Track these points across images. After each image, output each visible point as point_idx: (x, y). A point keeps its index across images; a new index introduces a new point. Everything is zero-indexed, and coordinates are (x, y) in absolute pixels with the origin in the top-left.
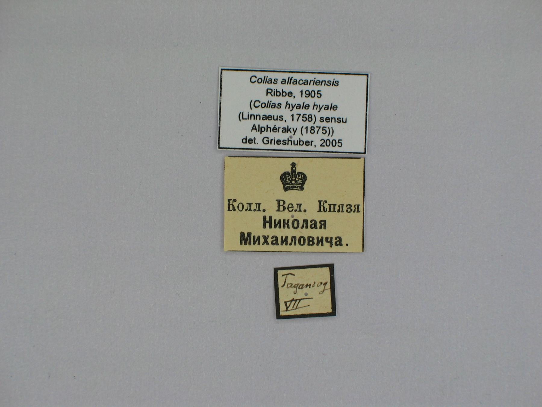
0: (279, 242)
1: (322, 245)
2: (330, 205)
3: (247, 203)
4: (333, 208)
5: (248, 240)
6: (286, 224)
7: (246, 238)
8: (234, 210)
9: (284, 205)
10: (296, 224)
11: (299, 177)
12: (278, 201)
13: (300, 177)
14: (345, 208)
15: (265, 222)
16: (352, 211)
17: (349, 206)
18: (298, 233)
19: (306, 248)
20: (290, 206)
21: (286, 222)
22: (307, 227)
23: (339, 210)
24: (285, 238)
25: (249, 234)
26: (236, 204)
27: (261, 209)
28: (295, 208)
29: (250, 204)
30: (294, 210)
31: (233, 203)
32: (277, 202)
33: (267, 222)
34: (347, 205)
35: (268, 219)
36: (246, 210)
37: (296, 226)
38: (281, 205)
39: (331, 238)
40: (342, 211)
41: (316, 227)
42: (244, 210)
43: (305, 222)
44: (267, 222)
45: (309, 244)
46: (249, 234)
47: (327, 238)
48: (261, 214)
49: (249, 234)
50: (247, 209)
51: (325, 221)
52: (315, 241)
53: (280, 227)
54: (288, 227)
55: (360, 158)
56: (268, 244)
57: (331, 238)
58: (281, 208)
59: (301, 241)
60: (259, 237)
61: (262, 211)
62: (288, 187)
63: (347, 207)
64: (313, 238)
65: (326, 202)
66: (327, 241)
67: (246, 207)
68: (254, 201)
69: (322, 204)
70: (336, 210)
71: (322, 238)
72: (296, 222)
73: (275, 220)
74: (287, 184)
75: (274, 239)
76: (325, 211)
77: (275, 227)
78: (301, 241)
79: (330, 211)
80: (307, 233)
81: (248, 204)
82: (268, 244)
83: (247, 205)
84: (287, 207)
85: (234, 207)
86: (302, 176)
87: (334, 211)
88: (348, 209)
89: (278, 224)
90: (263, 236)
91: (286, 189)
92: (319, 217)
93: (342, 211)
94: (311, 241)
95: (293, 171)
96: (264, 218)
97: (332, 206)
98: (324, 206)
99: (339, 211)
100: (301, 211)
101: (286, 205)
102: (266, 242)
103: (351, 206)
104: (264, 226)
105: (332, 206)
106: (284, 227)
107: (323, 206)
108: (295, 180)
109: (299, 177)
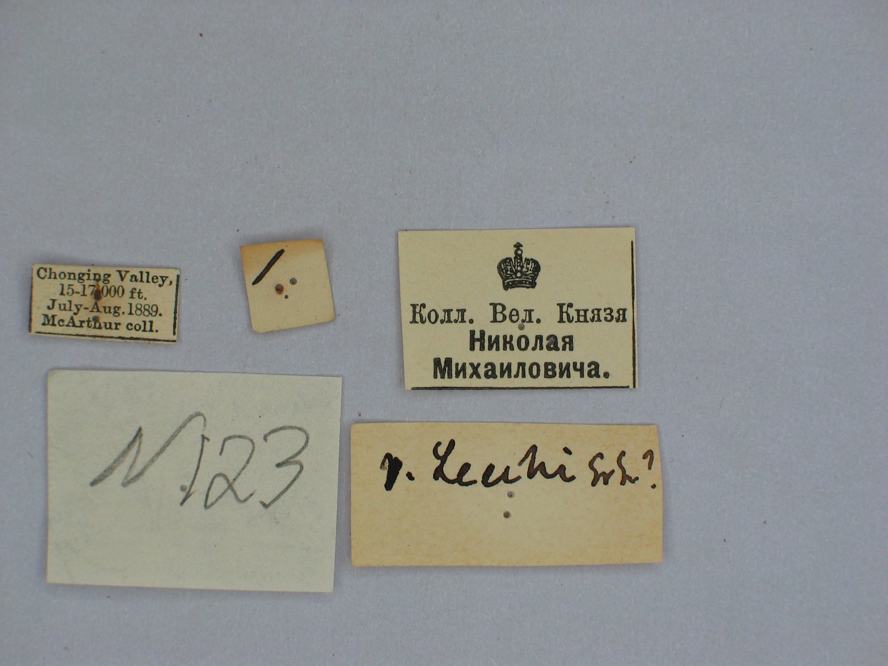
1: (569, 376)
2: (578, 311)
3: (525, 310)
4: (583, 316)
5: (438, 370)
6: (508, 342)
7: (443, 367)
8: (423, 322)
12: (494, 305)
13: (529, 266)
14: (603, 315)
15: (473, 340)
18: (529, 357)
19: (542, 381)
20: (514, 313)
21: (508, 339)
22: (541, 348)
23: (594, 317)
24: (566, 365)
25: (448, 361)
26: (425, 312)
27: (467, 318)
29: (448, 311)
32: (492, 307)
33: (478, 340)
35: (477, 336)
37: (523, 346)
38: (498, 311)
40: (599, 320)
41: (556, 348)
44: (477, 340)
45: (547, 376)
46: (438, 362)
48: (466, 328)
50: (443, 319)
51: (571, 337)
52: (557, 370)
53: (498, 349)
54: (512, 348)
56: (479, 376)
57: (582, 364)
60: (464, 365)
62: (510, 282)
64: (554, 365)
67: (441, 315)
70: (588, 319)
73: (490, 337)
75: (489, 367)
76: (570, 321)
77: (490, 348)
78: (532, 370)
79: (579, 321)
80: (543, 356)
82: (479, 376)
83: (525, 312)
87: (586, 321)
88: (607, 316)
89: (494, 343)
91: (506, 287)
92: (562, 331)
93: (599, 320)
95: (518, 257)
96: (472, 333)
97: (582, 313)
98: (568, 312)
99: (592, 320)
100: (465, 322)
101: (507, 313)
102: (475, 373)
104: (472, 348)
105: (582, 313)
106: (505, 348)
108: (521, 271)
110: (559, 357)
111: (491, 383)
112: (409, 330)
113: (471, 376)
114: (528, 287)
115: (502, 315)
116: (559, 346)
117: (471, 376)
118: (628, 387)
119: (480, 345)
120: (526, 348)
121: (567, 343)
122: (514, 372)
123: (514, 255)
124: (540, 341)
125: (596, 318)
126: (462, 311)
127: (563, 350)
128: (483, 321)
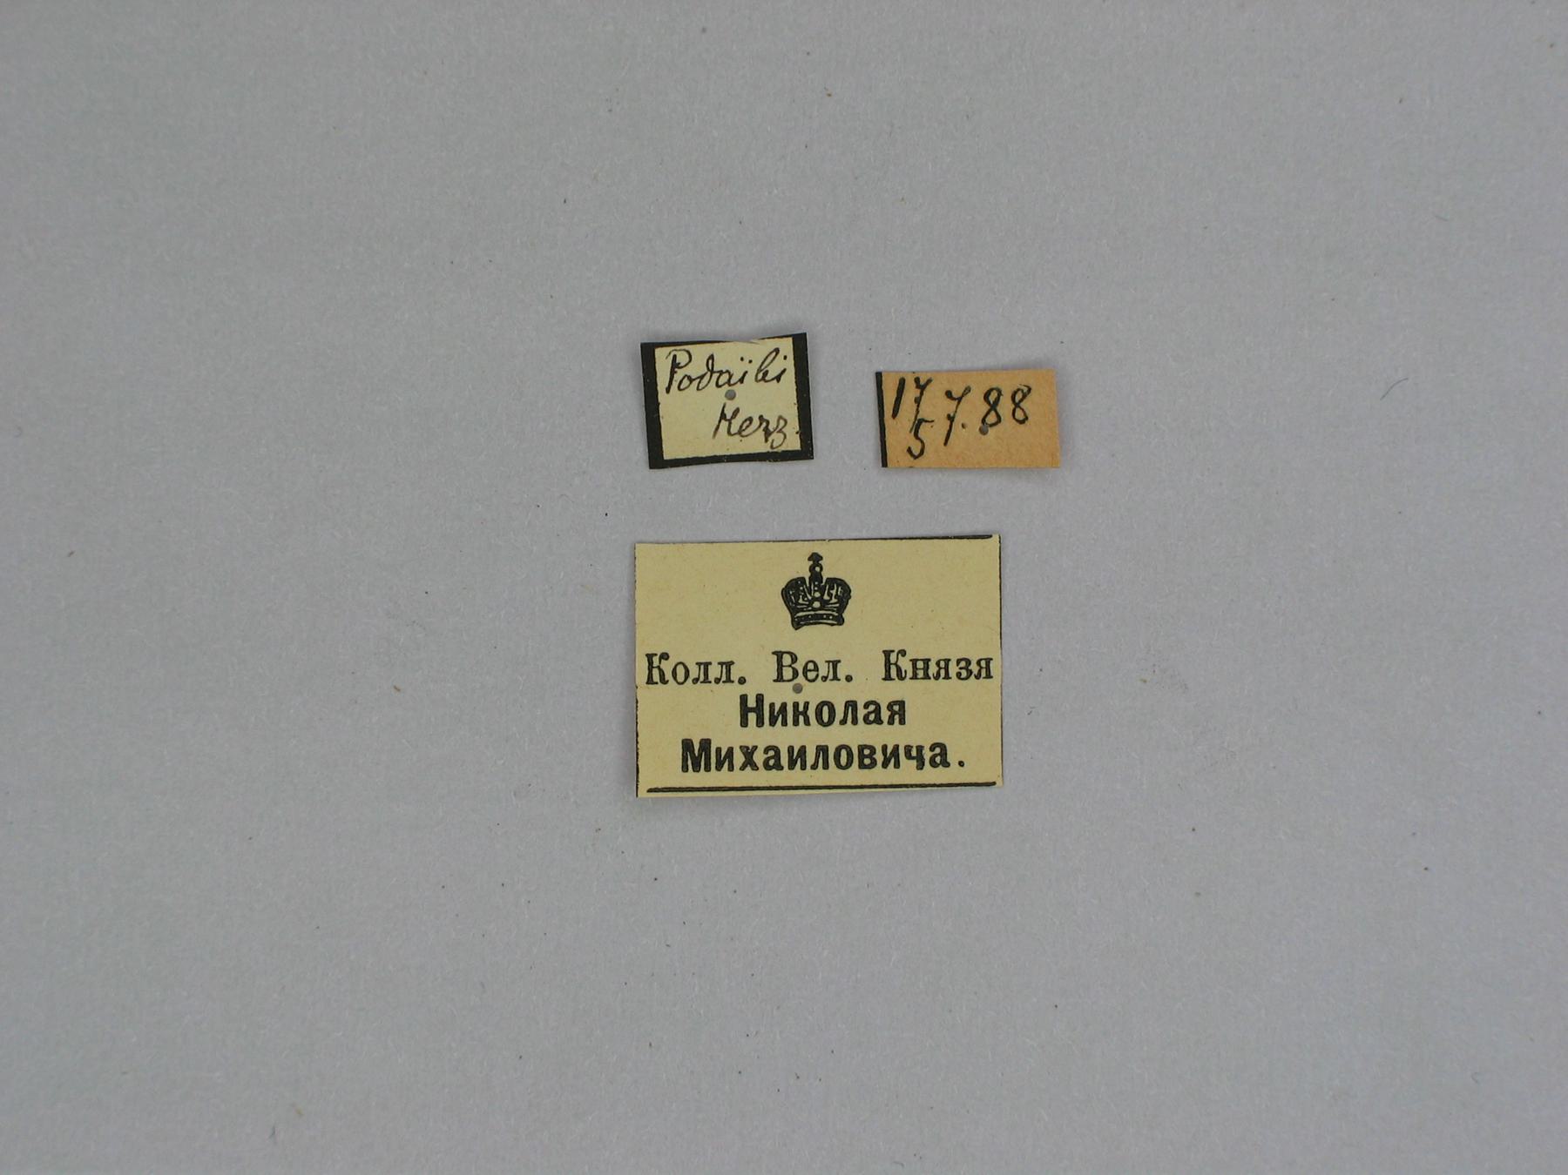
0: (784, 761)
1: (897, 765)
2: (914, 662)
4: (921, 669)
6: (800, 714)
7: (696, 755)
8: (664, 681)
10: (825, 714)
12: (779, 655)
13: (834, 592)
14: (953, 669)
15: (745, 710)
16: (973, 676)
17: (963, 664)
18: (835, 736)
19: (854, 775)
20: (811, 666)
21: (801, 708)
22: (855, 722)
24: (799, 750)
25: (705, 744)
27: (735, 676)
28: (823, 671)
30: (820, 678)
32: (776, 657)
33: (752, 710)
35: (752, 703)
36: (696, 681)
37: (826, 718)
39: (920, 749)
40: (947, 677)
41: (878, 721)
42: (690, 680)
43: (850, 708)
45: (862, 766)
47: (908, 749)
48: (736, 690)
49: (705, 744)
52: (879, 757)
53: (785, 723)
54: (807, 722)
55: (991, 536)
57: (920, 749)
59: (843, 757)
60: (730, 751)
65: (903, 653)
66: (909, 756)
68: (715, 657)
69: (893, 658)
71: (896, 748)
72: (825, 709)
74: (802, 610)
76: (901, 677)
77: (773, 723)
78: (843, 757)
79: (915, 677)
81: (699, 664)
82: (755, 767)
84: (800, 672)
85: (662, 674)
86: (840, 589)
87: (927, 677)
89: (778, 715)
90: (741, 747)
91: (797, 624)
92: (886, 693)
94: (866, 757)
95: (816, 576)
96: (744, 699)
97: (920, 665)
99: (937, 677)
101: (799, 666)
102: (749, 762)
103: (968, 662)
104: (744, 723)
105: (920, 665)
106: (796, 723)
107: (896, 664)
108: (821, 599)
111: (775, 778)
113: (743, 768)
114: (832, 625)
117: (743, 768)
120: (831, 722)
121: (896, 713)
122: (810, 759)
123: (809, 574)
125: (983, 673)
126: (728, 665)
128: (762, 682)
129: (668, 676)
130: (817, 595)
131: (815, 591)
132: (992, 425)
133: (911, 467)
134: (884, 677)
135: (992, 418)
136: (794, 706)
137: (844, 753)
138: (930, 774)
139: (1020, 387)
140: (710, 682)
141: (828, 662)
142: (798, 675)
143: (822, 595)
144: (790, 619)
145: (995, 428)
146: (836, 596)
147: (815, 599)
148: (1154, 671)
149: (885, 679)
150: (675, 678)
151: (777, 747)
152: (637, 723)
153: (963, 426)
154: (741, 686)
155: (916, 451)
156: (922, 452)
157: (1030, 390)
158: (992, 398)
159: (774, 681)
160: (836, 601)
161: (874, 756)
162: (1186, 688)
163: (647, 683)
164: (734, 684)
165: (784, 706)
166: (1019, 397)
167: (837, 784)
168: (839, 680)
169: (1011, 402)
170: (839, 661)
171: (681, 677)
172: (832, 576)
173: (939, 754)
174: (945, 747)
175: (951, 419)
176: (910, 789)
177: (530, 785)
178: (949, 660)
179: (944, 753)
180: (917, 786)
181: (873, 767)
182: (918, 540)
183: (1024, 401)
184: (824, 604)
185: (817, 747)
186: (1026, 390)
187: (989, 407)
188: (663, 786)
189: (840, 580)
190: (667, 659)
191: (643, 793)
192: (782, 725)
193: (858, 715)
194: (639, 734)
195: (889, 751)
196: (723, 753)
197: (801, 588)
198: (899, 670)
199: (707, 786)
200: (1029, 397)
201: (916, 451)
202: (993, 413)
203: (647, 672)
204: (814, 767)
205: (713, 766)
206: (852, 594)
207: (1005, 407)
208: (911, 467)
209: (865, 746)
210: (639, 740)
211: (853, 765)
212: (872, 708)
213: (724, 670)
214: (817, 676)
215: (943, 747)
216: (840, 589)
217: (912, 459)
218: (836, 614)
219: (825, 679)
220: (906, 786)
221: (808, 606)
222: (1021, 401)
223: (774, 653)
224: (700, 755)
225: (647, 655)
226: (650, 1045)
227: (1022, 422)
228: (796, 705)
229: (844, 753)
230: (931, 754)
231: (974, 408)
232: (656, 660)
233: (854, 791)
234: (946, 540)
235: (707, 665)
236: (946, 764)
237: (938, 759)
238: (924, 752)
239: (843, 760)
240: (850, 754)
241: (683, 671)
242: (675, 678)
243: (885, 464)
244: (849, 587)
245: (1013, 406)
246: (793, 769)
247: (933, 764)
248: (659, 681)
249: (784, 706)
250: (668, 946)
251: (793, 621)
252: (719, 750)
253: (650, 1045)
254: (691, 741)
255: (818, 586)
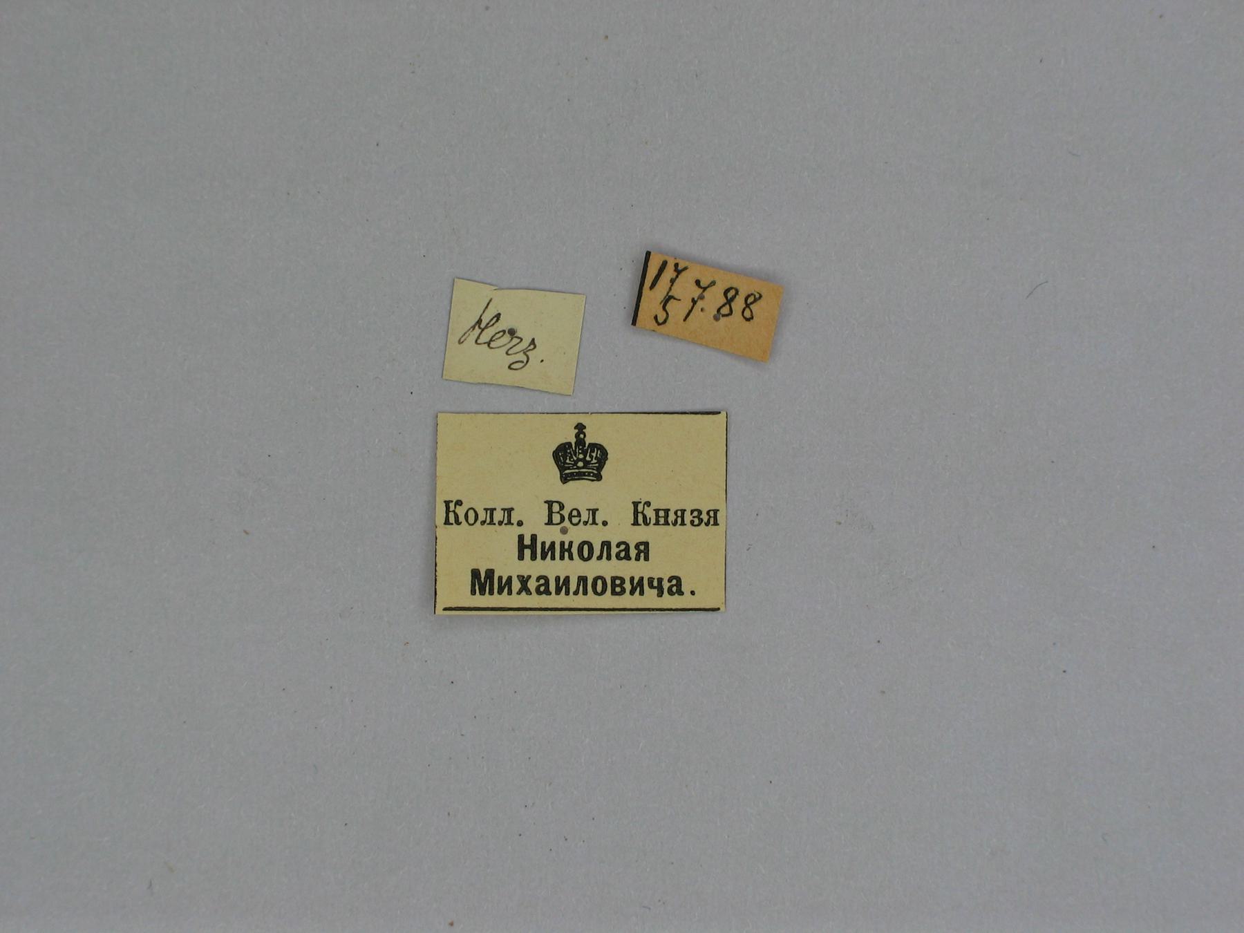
1: (642, 593)
2: (657, 511)
4: (663, 517)
6: (566, 550)
7: (482, 581)
8: (458, 522)
9: (561, 512)
10: (585, 551)
11: (593, 454)
12: (550, 504)
13: (594, 455)
14: (688, 518)
15: (521, 547)
16: (703, 523)
17: (695, 514)
18: (593, 569)
19: (608, 600)
20: (575, 513)
21: (566, 546)
22: (609, 558)
25: (490, 573)
26: (461, 511)
27: (514, 520)
28: (584, 517)
30: (582, 523)
31: (455, 508)
32: (547, 505)
33: (527, 547)
34: (692, 512)
35: (527, 541)
36: (483, 523)
37: (586, 554)
39: (660, 580)
40: (683, 523)
41: (628, 557)
42: (479, 522)
43: (605, 547)
45: (614, 593)
47: (651, 580)
48: (515, 531)
49: (490, 573)
51: (646, 544)
52: (628, 586)
53: (553, 558)
54: (571, 558)
55: (720, 413)
57: (660, 580)
58: (556, 518)
59: (599, 585)
60: (510, 579)
61: (515, 524)
63: (691, 514)
65: (648, 504)
66: (651, 586)
68: (499, 505)
69: (640, 508)
70: (670, 522)
71: (641, 579)
72: (586, 547)
74: (569, 468)
76: (646, 523)
77: (544, 557)
78: (599, 585)
79: (657, 523)
81: (486, 510)
82: (529, 592)
86: (599, 452)
87: (667, 523)
89: (548, 551)
90: (518, 576)
91: (565, 479)
92: (634, 535)
94: (617, 585)
95: (580, 442)
96: (521, 538)
97: (662, 513)
99: (675, 523)
101: (566, 513)
102: (524, 588)
103: (700, 512)
104: (521, 557)
105: (662, 513)
106: (562, 558)
107: (642, 513)
108: (584, 460)
109: (593, 454)
110: (630, 569)
111: (544, 601)
112: (443, 532)
113: (519, 593)
114: (593, 480)
115: (559, 516)
116: (631, 555)
117: (519, 593)
118: (719, 609)
119: (531, 554)
120: (590, 558)
121: (642, 551)
122: (573, 587)
124: (607, 548)
126: (509, 511)
127: (636, 560)
128: (536, 524)
129: (462, 518)
130: (581, 456)
131: (579, 453)
132: (723, 316)
133: (654, 331)
134: (632, 523)
135: (725, 310)
136: (561, 545)
137: (600, 582)
138: (668, 601)
139: (753, 292)
140: (495, 524)
141: (589, 510)
142: (564, 520)
143: (585, 456)
144: (559, 476)
145: (725, 318)
146: (596, 458)
147: (579, 460)
148: (847, 516)
149: (633, 525)
150: (467, 520)
151: (547, 577)
152: (436, 555)
153: (702, 310)
154: (519, 527)
155: (660, 320)
156: (665, 321)
157: (761, 296)
158: (730, 295)
159: (546, 524)
160: (596, 461)
161: (624, 586)
162: (873, 528)
163: (445, 524)
164: (513, 526)
165: (553, 544)
166: (751, 300)
167: (593, 607)
168: (597, 524)
169: (744, 302)
170: (597, 510)
171: (471, 520)
172: (593, 442)
173: (675, 585)
174: (680, 579)
175: (694, 302)
176: (652, 612)
177: (352, 608)
178: (685, 510)
179: (679, 584)
180: (657, 610)
181: (622, 594)
182: (662, 415)
183: (754, 304)
184: (586, 464)
185: (579, 577)
186: (757, 296)
187: (725, 301)
188: (456, 606)
189: (600, 445)
190: (461, 505)
191: (439, 610)
192: (551, 559)
193: (612, 553)
194: (438, 565)
195: (636, 581)
196: (504, 581)
197: (569, 451)
198: (645, 517)
199: (490, 606)
200: (758, 302)
201: (660, 320)
202: (728, 306)
203: (445, 515)
204: (576, 593)
205: (496, 591)
206: (608, 456)
207: (738, 304)
208: (654, 331)
209: (617, 577)
210: (437, 568)
211: (607, 592)
212: (623, 547)
213: (506, 515)
214: (580, 521)
215: (678, 579)
216: (599, 452)
217: (656, 324)
218: (595, 472)
219: (586, 523)
220: (648, 610)
221: (574, 465)
222: (752, 303)
223: (545, 502)
224: (486, 582)
225: (445, 502)
226: (449, 814)
227: (748, 320)
228: (562, 544)
229: (600, 582)
230: (669, 584)
231: (715, 298)
232: (452, 506)
233: (607, 612)
234: (684, 415)
235: (492, 510)
236: (680, 593)
237: (674, 589)
238: (663, 583)
239: (599, 588)
240: (604, 584)
241: (474, 515)
242: (467, 520)
243: (634, 323)
244: (606, 451)
245: (745, 306)
246: (559, 594)
247: (670, 592)
248: (454, 522)
249: (553, 544)
250: (462, 735)
251: (561, 477)
252: (500, 578)
253: (449, 814)
254: (478, 570)
255: (582, 449)
